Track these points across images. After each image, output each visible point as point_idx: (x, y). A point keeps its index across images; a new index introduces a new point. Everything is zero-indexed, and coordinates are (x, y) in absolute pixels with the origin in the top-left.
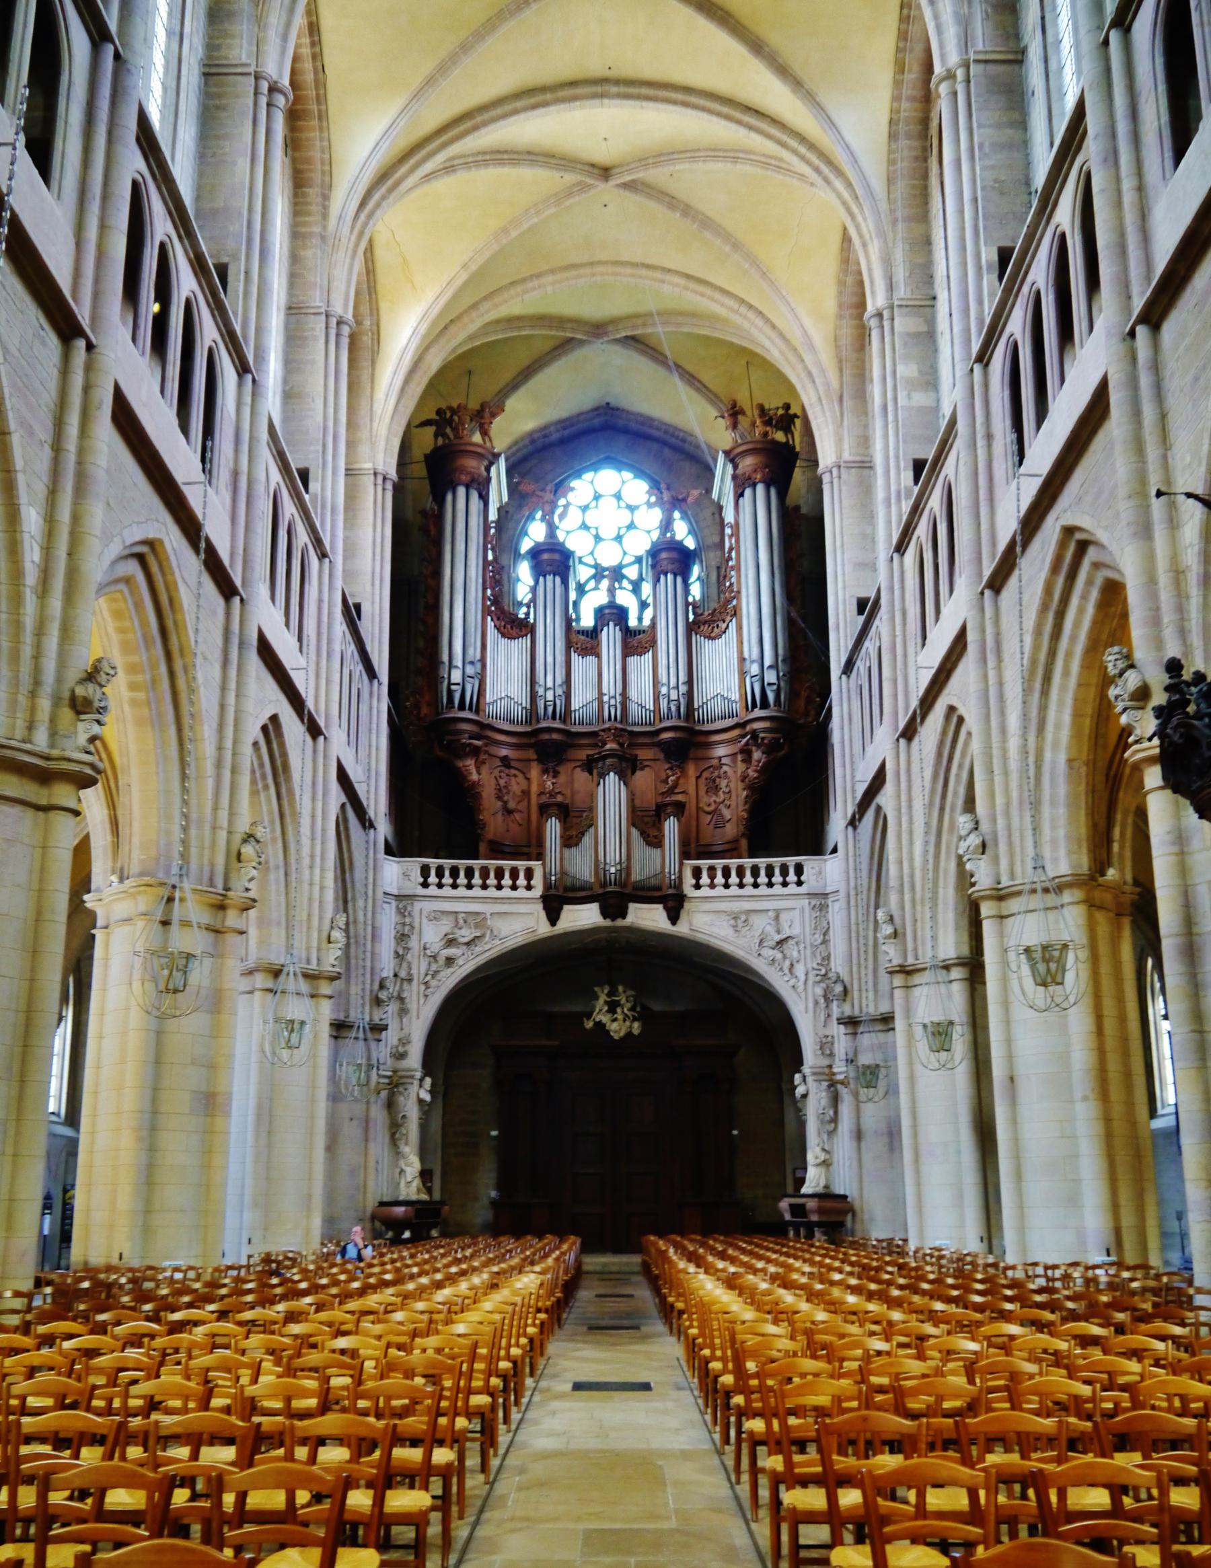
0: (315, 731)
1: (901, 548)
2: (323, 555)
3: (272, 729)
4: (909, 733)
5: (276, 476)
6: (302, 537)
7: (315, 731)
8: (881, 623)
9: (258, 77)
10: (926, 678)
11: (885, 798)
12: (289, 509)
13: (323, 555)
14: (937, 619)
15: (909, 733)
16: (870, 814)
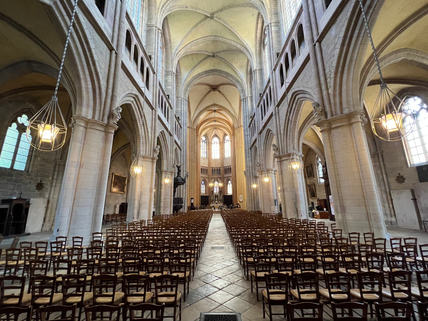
0: (171, 135)
1: (258, 106)
2: (171, 108)
3: (162, 133)
4: (260, 133)
5: (161, 94)
6: (167, 105)
7: (171, 135)
8: (255, 118)
9: (156, 27)
10: (264, 124)
11: (257, 144)
12: (165, 100)
13: (171, 108)
14: (265, 115)
15: (260, 133)
16: (254, 147)
